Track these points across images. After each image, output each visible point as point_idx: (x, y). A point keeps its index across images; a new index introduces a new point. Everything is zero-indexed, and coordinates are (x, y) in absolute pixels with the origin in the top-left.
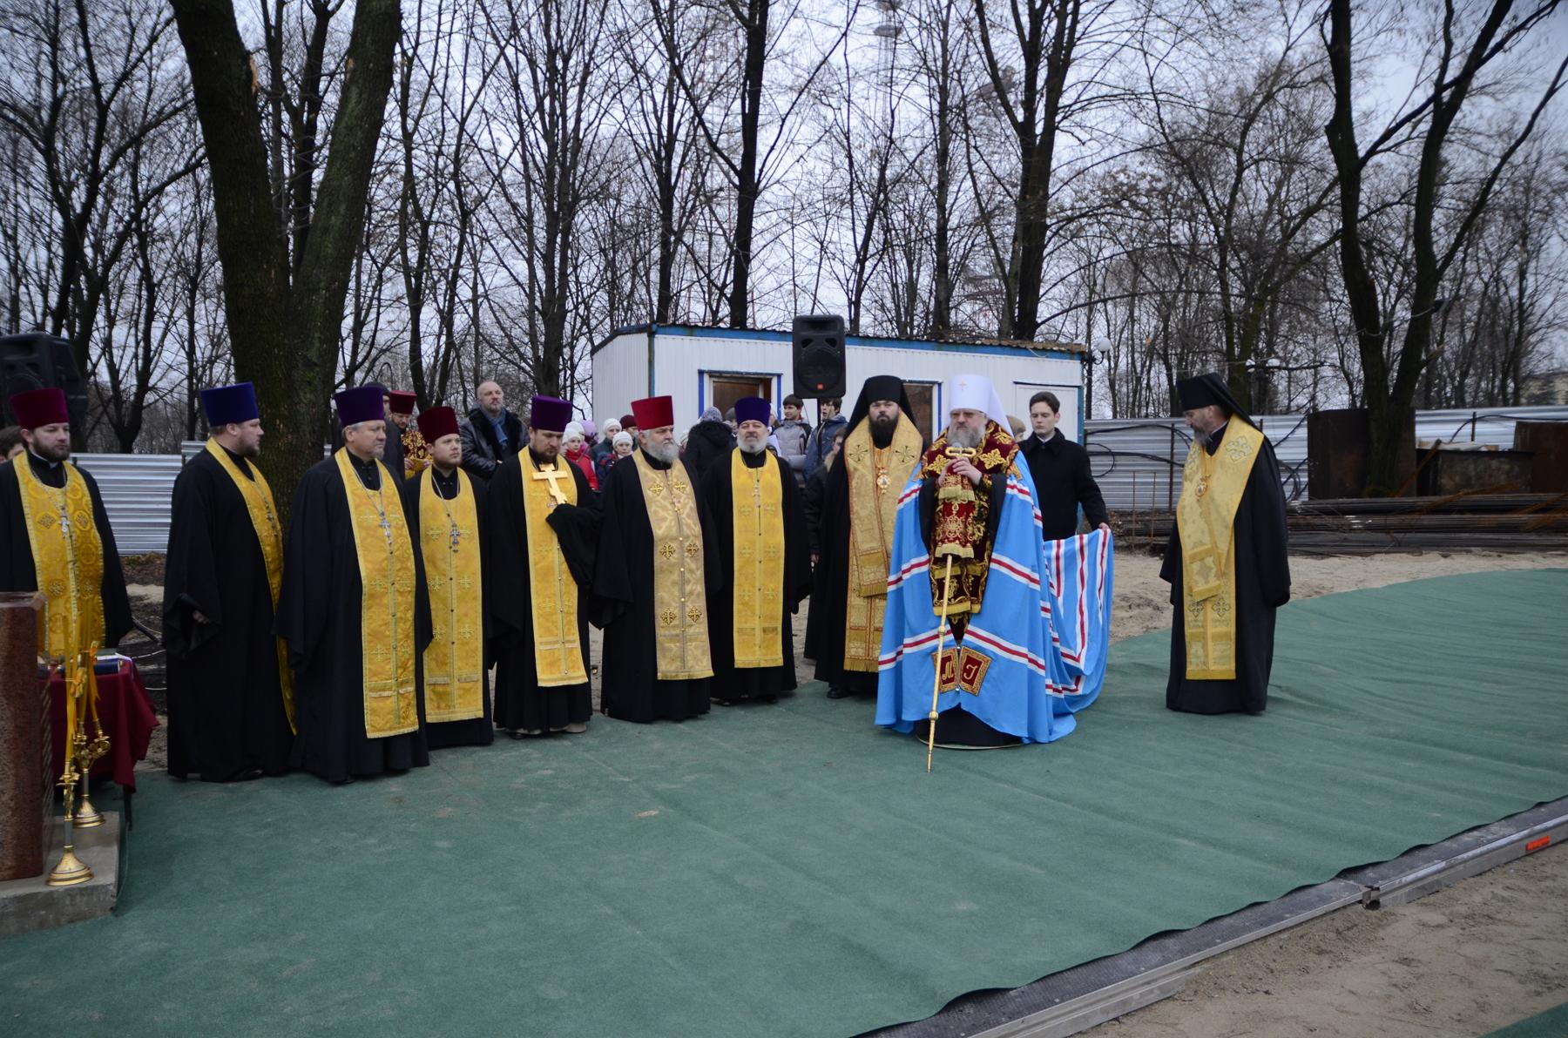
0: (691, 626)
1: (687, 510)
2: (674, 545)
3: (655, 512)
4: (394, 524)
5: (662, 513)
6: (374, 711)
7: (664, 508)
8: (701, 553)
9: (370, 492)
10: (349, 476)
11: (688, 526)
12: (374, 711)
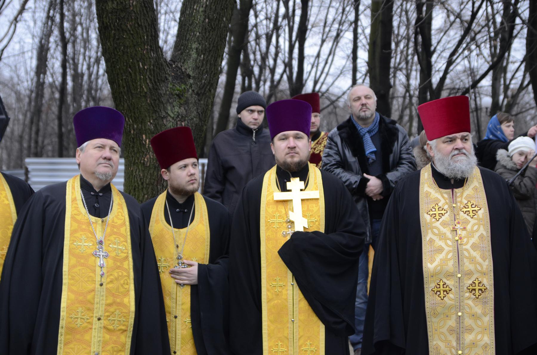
1: (475, 239)
2: (450, 283)
3: (431, 241)
5: (439, 243)
7: (442, 237)
8: (490, 295)
10: (74, 200)
11: (472, 260)
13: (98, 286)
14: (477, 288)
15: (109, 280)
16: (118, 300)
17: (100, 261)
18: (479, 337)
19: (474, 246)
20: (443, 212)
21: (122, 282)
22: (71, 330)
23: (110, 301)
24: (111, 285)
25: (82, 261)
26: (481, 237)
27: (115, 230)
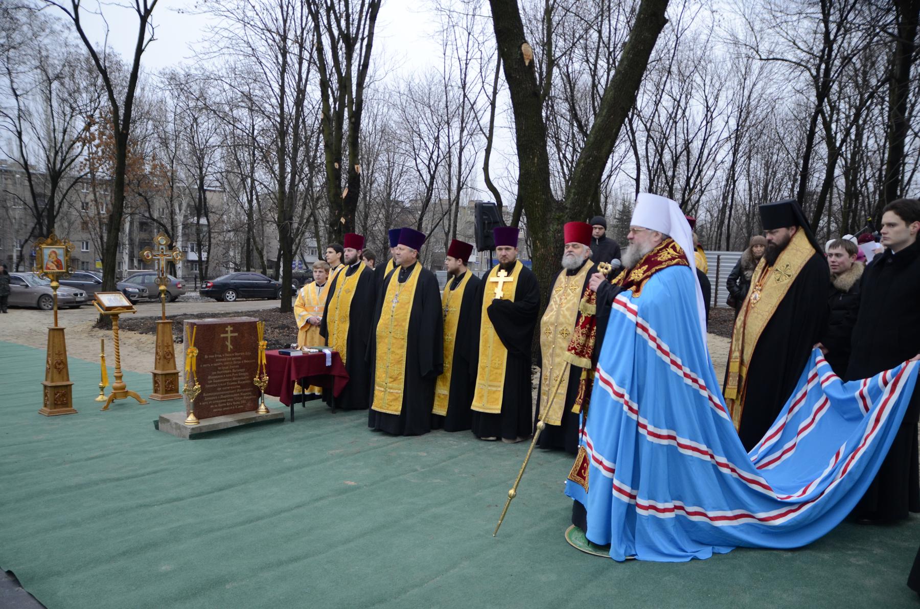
2: (552, 328)
11: (565, 316)
19: (568, 309)
23: (395, 324)
26: (574, 304)
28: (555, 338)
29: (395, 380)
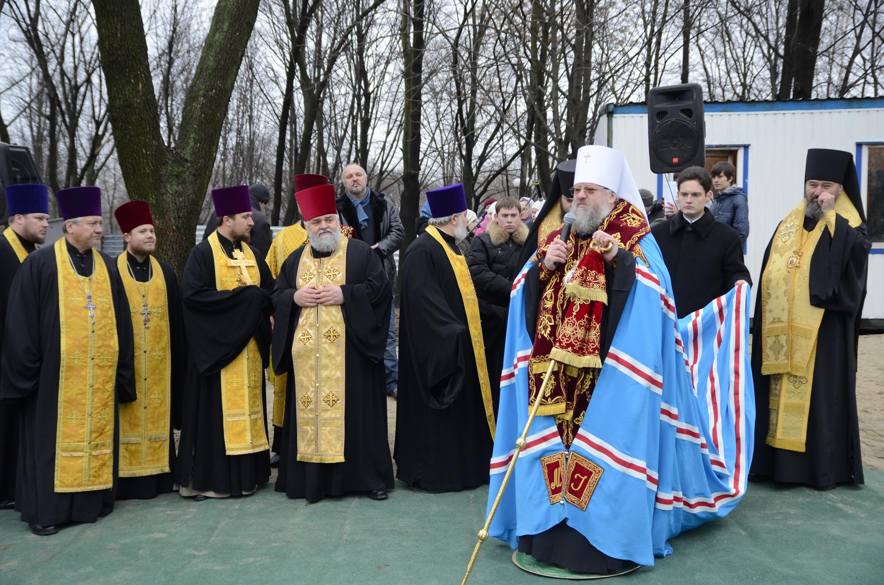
0: (326, 410)
4: (100, 306)
6: (63, 469)
8: (342, 339)
9: (82, 278)
10: (64, 262)
12: (63, 469)
13: (90, 333)
14: (332, 334)
15: (98, 327)
16: (106, 343)
17: (90, 313)
18: (333, 373)
20: (312, 276)
21: (108, 328)
22: (70, 368)
23: (100, 344)
24: (100, 332)
25: (76, 313)
27: (99, 286)
28: (318, 343)
29: (101, 434)
